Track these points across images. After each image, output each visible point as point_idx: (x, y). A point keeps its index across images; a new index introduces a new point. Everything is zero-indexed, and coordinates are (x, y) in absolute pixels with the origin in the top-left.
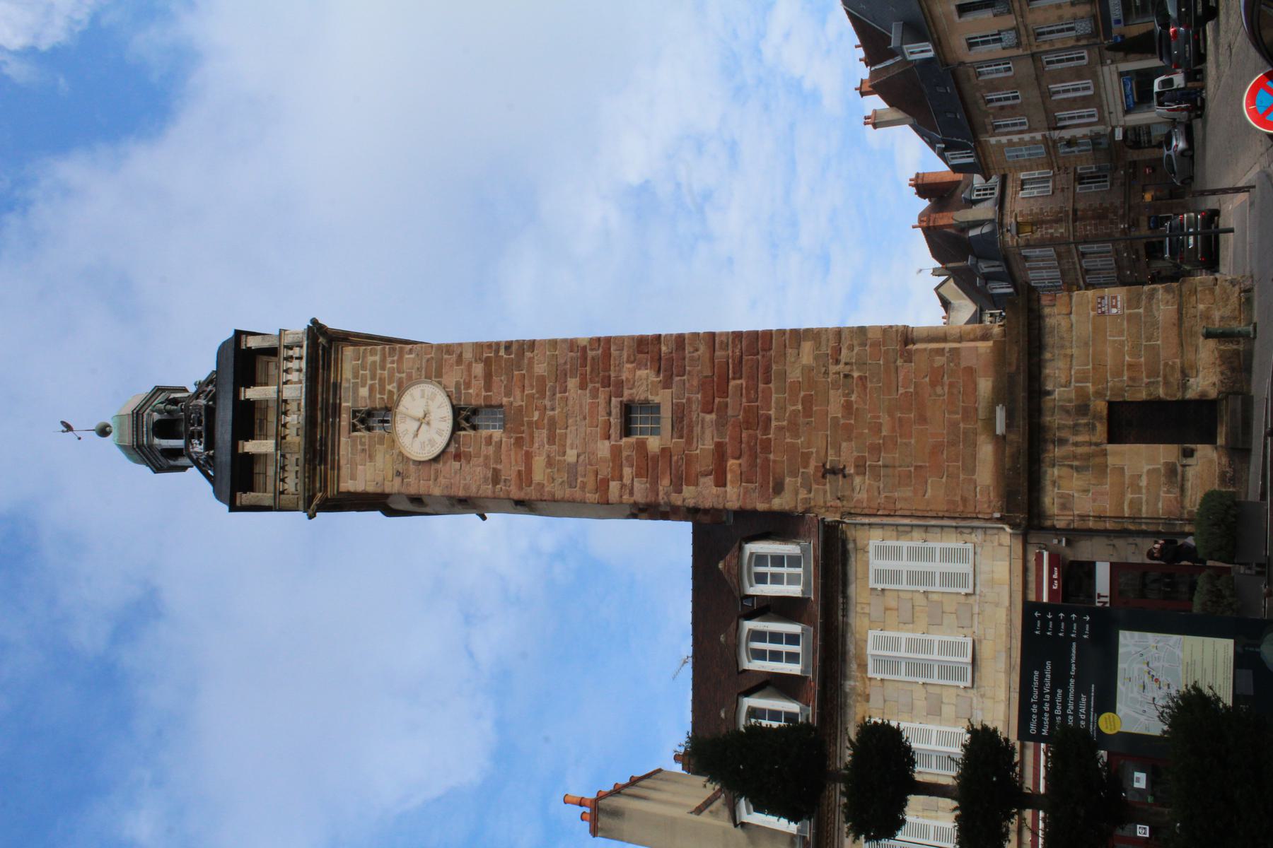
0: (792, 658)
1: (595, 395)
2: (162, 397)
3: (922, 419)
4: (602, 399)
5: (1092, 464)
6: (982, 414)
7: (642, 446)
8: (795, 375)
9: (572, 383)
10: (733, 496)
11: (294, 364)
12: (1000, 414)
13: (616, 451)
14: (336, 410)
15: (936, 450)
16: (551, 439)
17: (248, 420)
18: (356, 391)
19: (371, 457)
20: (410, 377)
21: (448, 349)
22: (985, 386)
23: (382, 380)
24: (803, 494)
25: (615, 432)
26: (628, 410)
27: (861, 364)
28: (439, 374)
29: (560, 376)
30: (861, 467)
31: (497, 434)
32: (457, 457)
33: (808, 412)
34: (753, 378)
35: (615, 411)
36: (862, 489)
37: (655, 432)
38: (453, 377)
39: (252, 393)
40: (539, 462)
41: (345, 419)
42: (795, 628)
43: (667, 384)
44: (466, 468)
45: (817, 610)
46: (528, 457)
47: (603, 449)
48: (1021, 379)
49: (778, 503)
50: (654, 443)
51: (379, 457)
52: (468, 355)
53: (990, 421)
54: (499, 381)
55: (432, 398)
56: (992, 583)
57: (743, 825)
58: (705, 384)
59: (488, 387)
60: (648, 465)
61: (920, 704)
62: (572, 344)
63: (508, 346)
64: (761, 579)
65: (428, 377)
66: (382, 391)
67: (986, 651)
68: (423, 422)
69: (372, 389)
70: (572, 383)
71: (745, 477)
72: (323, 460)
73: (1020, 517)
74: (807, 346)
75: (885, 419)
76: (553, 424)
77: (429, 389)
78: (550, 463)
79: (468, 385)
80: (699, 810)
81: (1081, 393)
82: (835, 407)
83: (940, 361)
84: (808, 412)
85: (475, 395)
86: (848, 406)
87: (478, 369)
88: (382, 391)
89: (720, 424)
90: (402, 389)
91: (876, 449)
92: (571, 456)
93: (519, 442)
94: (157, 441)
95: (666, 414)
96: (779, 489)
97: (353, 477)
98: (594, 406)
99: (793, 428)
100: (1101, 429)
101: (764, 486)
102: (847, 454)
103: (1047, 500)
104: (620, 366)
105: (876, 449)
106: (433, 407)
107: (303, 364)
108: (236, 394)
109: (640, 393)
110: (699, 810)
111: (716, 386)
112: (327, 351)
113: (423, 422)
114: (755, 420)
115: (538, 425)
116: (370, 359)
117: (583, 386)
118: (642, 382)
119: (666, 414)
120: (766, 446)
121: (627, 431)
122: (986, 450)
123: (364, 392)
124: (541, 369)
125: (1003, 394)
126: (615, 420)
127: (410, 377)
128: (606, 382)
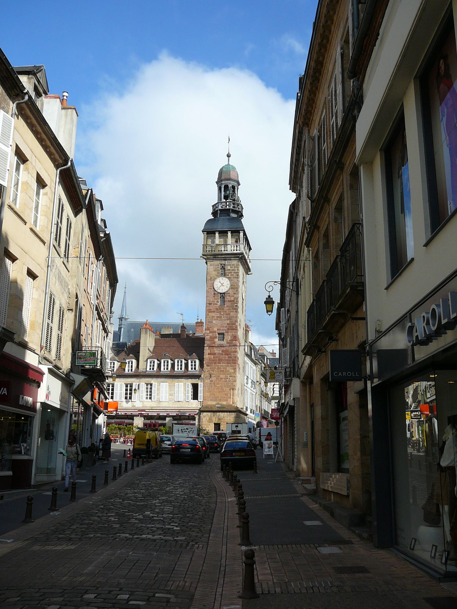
0: (178, 369)
1: (226, 327)
2: (235, 184)
3: (219, 392)
4: (225, 328)
5: (210, 420)
6: (220, 402)
7: (216, 337)
8: (228, 368)
9: (228, 321)
10: (206, 356)
11: (235, 249)
12: (219, 406)
13: (215, 332)
14: (225, 260)
15: (214, 395)
16: (217, 317)
17: (223, 233)
18: (230, 265)
19: (214, 270)
20: (232, 280)
21: (237, 291)
22: (224, 403)
23: (231, 273)
24: (207, 370)
25: (219, 332)
26: (223, 334)
27: (229, 381)
28: (232, 288)
29: (230, 319)
30: (211, 381)
31: (219, 304)
32: (214, 294)
33: (221, 371)
34: (228, 360)
35: (223, 332)
36: (208, 381)
37: (219, 340)
38: (231, 292)
39: (229, 234)
40: (213, 314)
41: (223, 262)
42: (183, 369)
43: (227, 343)
44: (212, 296)
45: (186, 374)
46: (214, 312)
47: (215, 329)
48: (224, 409)
49: (205, 365)
50: (216, 340)
51: (214, 273)
52: (235, 296)
53: (218, 404)
54: (229, 304)
55: (227, 287)
56: (192, 404)
57: (147, 360)
58: (227, 351)
59: (228, 301)
60: (212, 338)
61: (171, 392)
62: (236, 321)
63: (236, 306)
64: (192, 362)
65: (231, 285)
66: (229, 273)
67: (181, 403)
68: (222, 285)
69: (230, 270)
70: (228, 321)
71: (210, 359)
72: (214, 258)
73: (202, 410)
74: (233, 371)
75: (219, 385)
76: (220, 317)
77: (229, 286)
78: (213, 317)
79: (229, 296)
80: (149, 349)
81: (222, 419)
82: (222, 376)
83: (229, 395)
84: (221, 371)
85: (227, 298)
86: (222, 379)
87: (232, 299)
88: (229, 273)
89: (219, 354)
90: (229, 278)
91: (214, 384)
92: (214, 322)
93: (217, 309)
94: (223, 186)
95: (222, 342)
96: (208, 366)
97: (210, 265)
98: (223, 327)
99: (218, 368)
100: (216, 422)
101: (209, 363)
102: (214, 378)
103: (205, 413)
104: (231, 332)
105: (214, 384)
106: (225, 287)
107: (235, 252)
108: (229, 231)
109: (226, 337)
110: (149, 349)
111: (226, 353)
112: (238, 257)
113: (222, 285)
114: (220, 360)
115: (220, 314)
116: (236, 269)
117: (228, 324)
118: (228, 337)
119: (222, 342)
120: (215, 363)
121: (219, 334)
122: (214, 403)
123: (229, 268)
124: (232, 314)
125: (223, 407)
126: (221, 332)
127: (232, 280)
128: (228, 329)
